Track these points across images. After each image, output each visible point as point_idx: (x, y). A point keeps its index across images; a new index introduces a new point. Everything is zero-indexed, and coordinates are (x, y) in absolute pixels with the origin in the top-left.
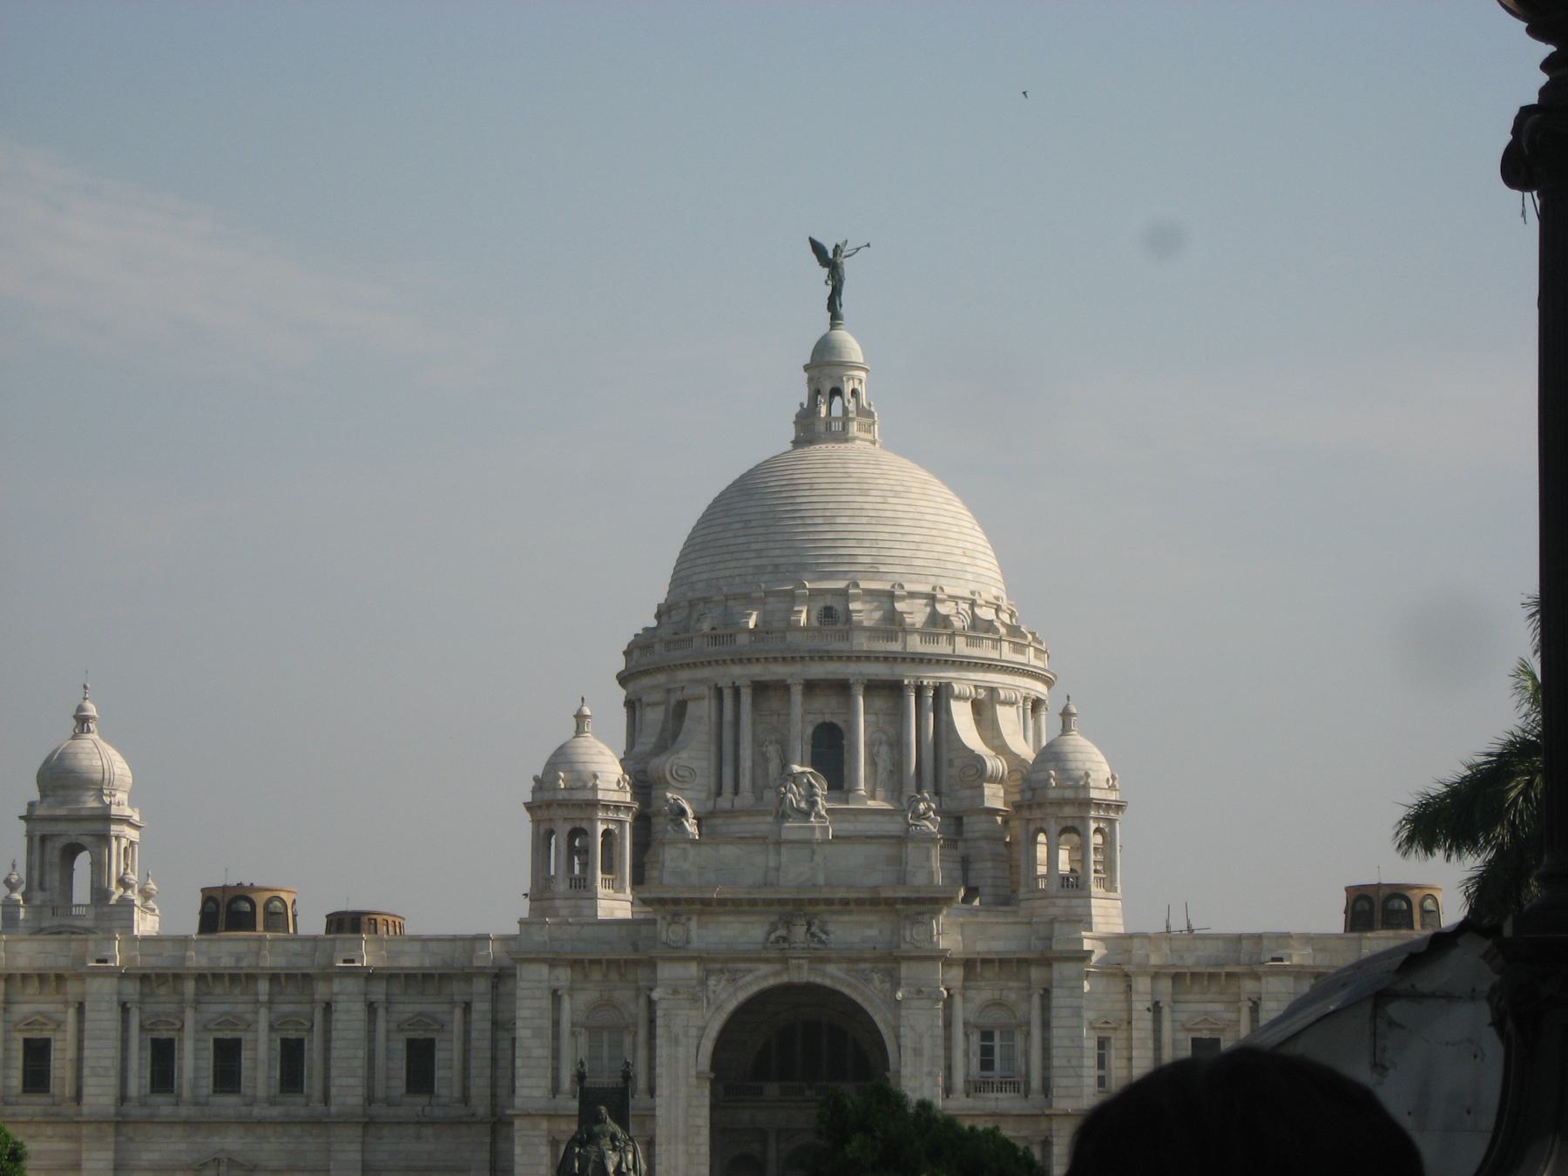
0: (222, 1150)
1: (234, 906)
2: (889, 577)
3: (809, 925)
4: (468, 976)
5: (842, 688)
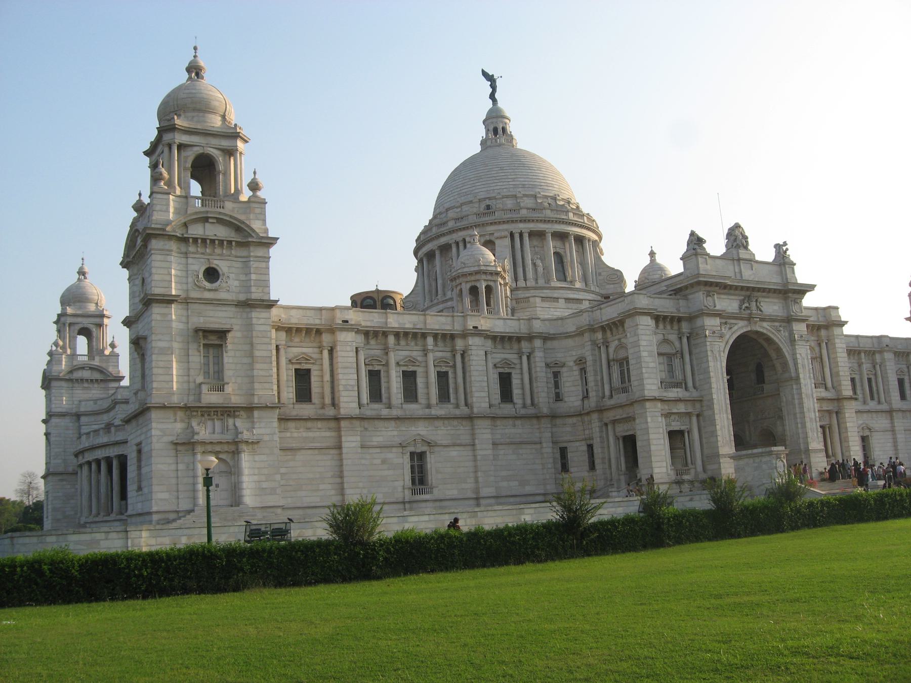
0: (419, 435)
1: (385, 301)
2: (565, 195)
3: (756, 301)
4: (530, 338)
5: (562, 237)
